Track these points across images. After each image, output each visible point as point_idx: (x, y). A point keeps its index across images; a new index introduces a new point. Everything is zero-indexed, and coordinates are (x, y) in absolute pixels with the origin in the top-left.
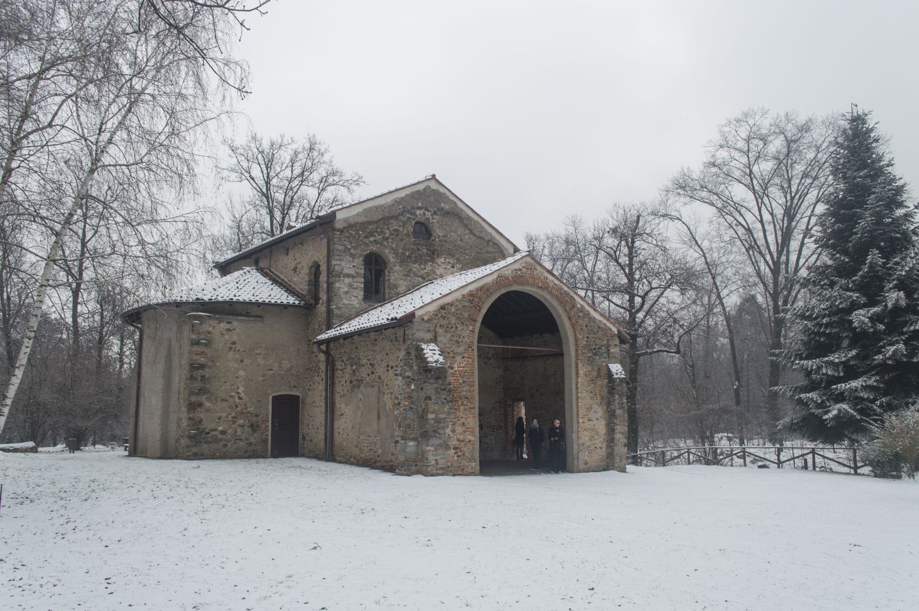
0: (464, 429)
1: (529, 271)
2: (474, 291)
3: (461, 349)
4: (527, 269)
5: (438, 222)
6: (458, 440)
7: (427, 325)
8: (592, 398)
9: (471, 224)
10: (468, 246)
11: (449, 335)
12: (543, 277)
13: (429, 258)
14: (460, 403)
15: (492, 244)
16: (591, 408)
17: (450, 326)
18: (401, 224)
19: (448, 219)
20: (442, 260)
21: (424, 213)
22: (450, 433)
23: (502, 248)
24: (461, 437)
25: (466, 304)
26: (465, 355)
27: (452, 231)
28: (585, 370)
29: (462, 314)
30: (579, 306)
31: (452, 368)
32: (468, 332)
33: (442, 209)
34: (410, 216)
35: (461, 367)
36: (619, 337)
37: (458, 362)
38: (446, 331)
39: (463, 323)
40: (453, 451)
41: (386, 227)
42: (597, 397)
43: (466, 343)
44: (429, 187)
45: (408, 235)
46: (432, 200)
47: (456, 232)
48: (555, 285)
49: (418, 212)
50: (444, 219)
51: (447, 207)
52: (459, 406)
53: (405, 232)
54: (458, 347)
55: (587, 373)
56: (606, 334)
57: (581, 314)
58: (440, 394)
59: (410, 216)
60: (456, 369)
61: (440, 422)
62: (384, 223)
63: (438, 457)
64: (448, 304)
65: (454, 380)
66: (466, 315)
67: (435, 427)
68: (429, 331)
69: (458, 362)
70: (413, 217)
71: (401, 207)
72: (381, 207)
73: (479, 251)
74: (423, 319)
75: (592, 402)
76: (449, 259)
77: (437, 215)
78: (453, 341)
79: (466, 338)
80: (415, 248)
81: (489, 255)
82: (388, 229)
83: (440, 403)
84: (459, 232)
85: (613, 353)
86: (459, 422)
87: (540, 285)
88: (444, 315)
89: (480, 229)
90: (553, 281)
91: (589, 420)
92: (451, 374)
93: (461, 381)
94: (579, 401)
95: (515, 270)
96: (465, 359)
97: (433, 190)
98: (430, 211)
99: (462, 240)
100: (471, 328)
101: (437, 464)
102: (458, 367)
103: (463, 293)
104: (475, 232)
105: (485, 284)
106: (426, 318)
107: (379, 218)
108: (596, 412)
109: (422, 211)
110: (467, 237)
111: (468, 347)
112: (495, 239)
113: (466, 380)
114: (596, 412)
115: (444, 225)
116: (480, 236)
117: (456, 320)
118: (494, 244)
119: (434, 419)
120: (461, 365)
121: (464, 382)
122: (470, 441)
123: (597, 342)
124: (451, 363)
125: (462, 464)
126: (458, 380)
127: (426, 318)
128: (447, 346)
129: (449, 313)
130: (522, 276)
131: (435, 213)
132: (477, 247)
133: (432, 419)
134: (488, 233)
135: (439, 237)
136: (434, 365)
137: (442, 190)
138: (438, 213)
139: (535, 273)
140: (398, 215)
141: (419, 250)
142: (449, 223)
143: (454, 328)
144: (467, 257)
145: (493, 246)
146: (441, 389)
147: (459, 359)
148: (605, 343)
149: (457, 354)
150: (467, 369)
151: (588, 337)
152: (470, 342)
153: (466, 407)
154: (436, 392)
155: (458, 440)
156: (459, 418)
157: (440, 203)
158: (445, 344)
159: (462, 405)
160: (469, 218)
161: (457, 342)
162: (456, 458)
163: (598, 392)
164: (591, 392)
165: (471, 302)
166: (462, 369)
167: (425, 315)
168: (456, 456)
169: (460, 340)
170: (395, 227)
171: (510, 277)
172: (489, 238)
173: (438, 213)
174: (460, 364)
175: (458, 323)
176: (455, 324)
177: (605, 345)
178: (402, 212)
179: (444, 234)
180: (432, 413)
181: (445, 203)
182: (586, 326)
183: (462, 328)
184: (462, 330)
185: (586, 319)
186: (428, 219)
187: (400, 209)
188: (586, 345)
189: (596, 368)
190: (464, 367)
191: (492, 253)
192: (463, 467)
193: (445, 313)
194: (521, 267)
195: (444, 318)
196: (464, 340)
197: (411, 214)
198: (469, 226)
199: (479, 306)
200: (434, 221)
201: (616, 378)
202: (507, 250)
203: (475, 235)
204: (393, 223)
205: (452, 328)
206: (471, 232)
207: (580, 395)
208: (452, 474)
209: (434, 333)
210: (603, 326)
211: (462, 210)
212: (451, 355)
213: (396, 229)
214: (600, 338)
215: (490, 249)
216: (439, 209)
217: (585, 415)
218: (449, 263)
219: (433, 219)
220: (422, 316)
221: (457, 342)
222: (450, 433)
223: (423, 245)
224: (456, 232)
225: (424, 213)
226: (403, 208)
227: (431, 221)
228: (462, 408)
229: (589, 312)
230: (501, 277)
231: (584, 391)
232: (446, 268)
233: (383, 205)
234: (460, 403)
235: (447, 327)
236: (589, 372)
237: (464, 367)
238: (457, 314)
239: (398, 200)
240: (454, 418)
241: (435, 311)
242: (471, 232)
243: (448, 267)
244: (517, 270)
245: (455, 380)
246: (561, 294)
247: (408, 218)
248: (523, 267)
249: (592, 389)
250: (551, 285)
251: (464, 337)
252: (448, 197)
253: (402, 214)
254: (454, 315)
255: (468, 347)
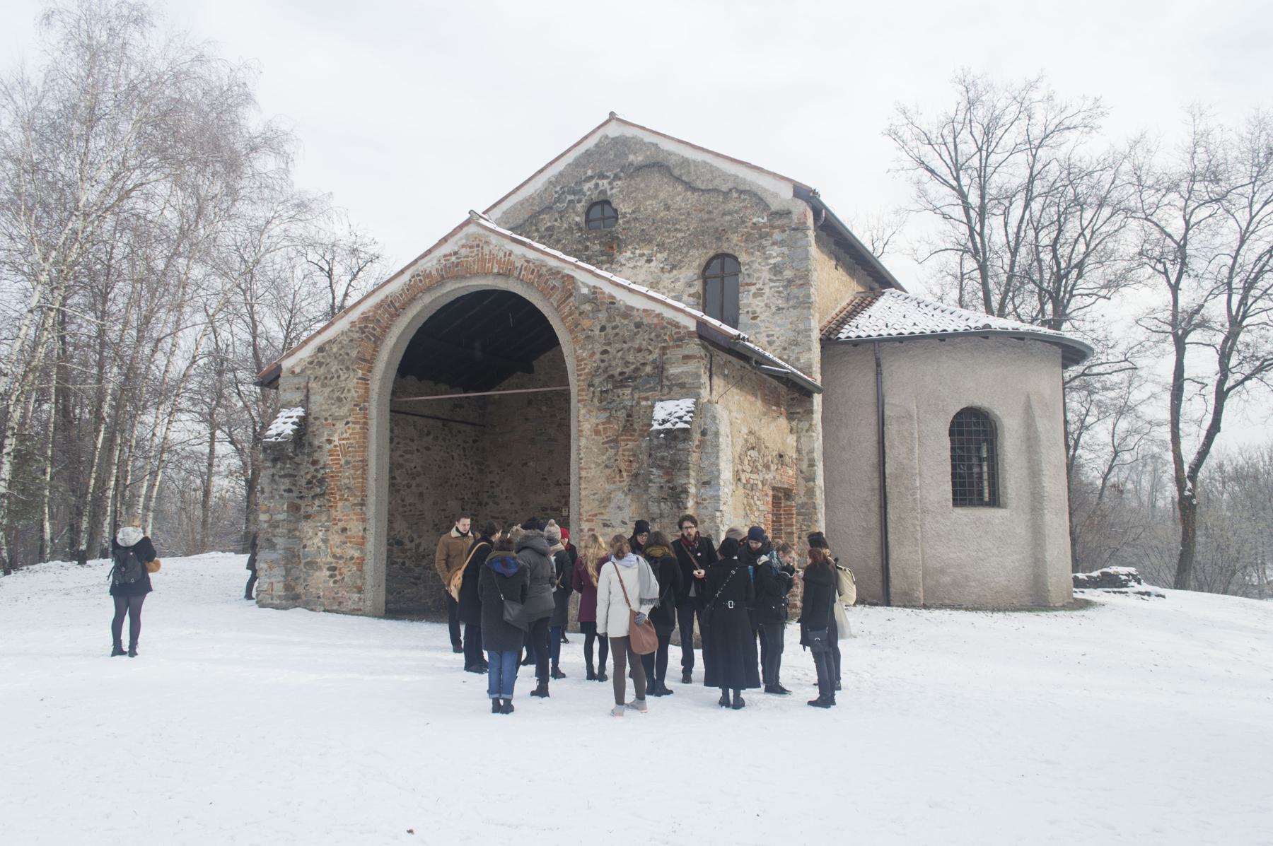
0: (343, 538)
1: (475, 249)
2: (369, 311)
3: (344, 411)
4: (471, 247)
5: (621, 192)
6: (334, 556)
7: (296, 380)
8: (610, 479)
9: (689, 172)
10: (680, 214)
11: (328, 390)
12: (501, 254)
13: (604, 258)
14: (338, 498)
15: (735, 195)
16: (609, 499)
17: (329, 377)
18: (557, 215)
19: (639, 179)
20: (629, 254)
21: (597, 185)
22: (320, 544)
23: (764, 196)
24: (338, 551)
25: (356, 336)
26: (349, 420)
27: (650, 197)
28: (594, 421)
29: (348, 354)
30: (585, 291)
31: (329, 441)
32: (355, 381)
33: (631, 164)
34: (572, 197)
35: (343, 439)
36: (701, 337)
37: (339, 431)
38: (324, 386)
39: (348, 369)
40: (328, 573)
41: (534, 228)
42: (621, 476)
43: (353, 398)
44: (607, 137)
45: (570, 230)
46: (612, 157)
47: (656, 197)
48: (528, 262)
49: (586, 187)
50: (633, 182)
51: (640, 158)
52: (336, 502)
53: (565, 226)
54: (340, 407)
55: (601, 427)
56: (658, 336)
57: (587, 307)
58: (277, 485)
59: (572, 197)
60: (336, 443)
61: (278, 526)
62: (531, 223)
63: (273, 580)
64: (330, 341)
65: (332, 460)
66: (354, 354)
67: (268, 532)
68: (298, 389)
69: (339, 431)
70: (577, 197)
71: (558, 189)
72: (527, 200)
73: (706, 216)
74: (293, 372)
75: (609, 487)
76: (640, 249)
77: (620, 179)
78: (333, 399)
79: (353, 391)
80: (580, 247)
81: (728, 218)
82: (537, 230)
83: (278, 497)
84: (662, 195)
85: (677, 376)
86: (336, 527)
87: (495, 271)
88: (323, 360)
89: (709, 176)
90: (525, 256)
91: (605, 525)
92: (329, 451)
93: (342, 462)
94: (583, 486)
95: (445, 256)
96: (350, 425)
97: (613, 139)
98: (608, 177)
99: (668, 208)
100: (360, 373)
101: (272, 590)
102: (340, 440)
103: (351, 320)
104: (699, 184)
105: (387, 296)
106: (297, 370)
107: (526, 217)
108: (620, 508)
109: (593, 182)
110: (678, 198)
111: (355, 405)
112: (744, 181)
113: (349, 459)
114: (620, 508)
115: (632, 192)
116: (710, 187)
117: (338, 365)
118: (741, 192)
119: (268, 522)
120: (345, 436)
121: (347, 463)
122: (352, 558)
123: (631, 358)
124: (328, 435)
125: (340, 595)
126: (340, 460)
127: (297, 370)
128: (323, 407)
129: (329, 356)
130: (458, 264)
131: (616, 177)
132: (701, 210)
133: (265, 522)
134: (725, 177)
135: (624, 216)
136: (273, 440)
137: (629, 132)
138: (622, 174)
139: (486, 250)
140: (555, 202)
141: (587, 248)
142: (642, 185)
143: (335, 379)
144: (679, 235)
145: (740, 197)
146: (280, 477)
147: (340, 425)
148: (655, 355)
149: (336, 419)
150: (352, 441)
151: (605, 352)
152: (358, 397)
153: (347, 503)
154: (272, 481)
155: (334, 556)
156: (335, 521)
157: (626, 155)
158: (321, 405)
159: (340, 500)
160: (685, 162)
161: (339, 399)
162: (331, 584)
163: (623, 466)
164: (606, 466)
165: (362, 330)
166: (345, 442)
167: (297, 365)
168: (332, 580)
169: (342, 396)
170: (549, 224)
171: (434, 272)
172: (731, 185)
173: (622, 174)
174: (342, 434)
175: (342, 370)
176: (337, 371)
177: (654, 361)
178: (560, 196)
179: (633, 208)
180: (265, 512)
181: (635, 153)
182: (603, 329)
183: (346, 376)
184: (346, 380)
185: (602, 316)
186: (604, 192)
187: (556, 192)
188: (598, 368)
189: (622, 414)
190: (348, 439)
191: (736, 212)
192: (341, 600)
193: (323, 357)
194: (456, 248)
195: (320, 364)
196: (349, 395)
197: (574, 193)
198: (684, 178)
199: (374, 335)
200: (614, 191)
201: (659, 432)
202: (775, 195)
203: (694, 189)
204: (544, 219)
205: (332, 378)
206: (690, 187)
207: (584, 474)
208: (322, 608)
209: (305, 391)
210: (656, 321)
211: (670, 154)
212: (330, 421)
213: (549, 227)
214: (639, 350)
215: (731, 206)
216: (623, 169)
217: (595, 515)
218: (642, 255)
219: (612, 189)
220: (293, 367)
221: (339, 399)
222: (320, 544)
223: (595, 238)
224: (656, 197)
225: (597, 185)
226: (561, 189)
227: (609, 193)
228: (340, 504)
229: (614, 298)
230: (418, 275)
231: (593, 466)
232: (635, 267)
233: (530, 196)
234: (338, 498)
235: (326, 378)
236: (603, 423)
237: (348, 439)
238: (341, 355)
239: (553, 179)
240: (327, 521)
241: (311, 356)
242: (690, 187)
243: (639, 264)
244: (450, 255)
245: (336, 460)
246: (540, 276)
247: (570, 201)
248: (463, 246)
249: (609, 459)
250: (518, 264)
251: (349, 391)
252: (642, 140)
253: (559, 200)
254: (336, 358)
255: (355, 405)
